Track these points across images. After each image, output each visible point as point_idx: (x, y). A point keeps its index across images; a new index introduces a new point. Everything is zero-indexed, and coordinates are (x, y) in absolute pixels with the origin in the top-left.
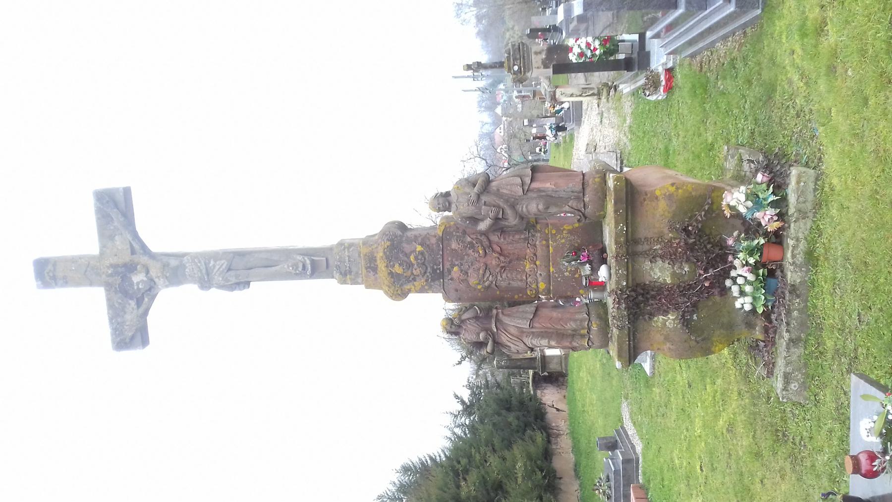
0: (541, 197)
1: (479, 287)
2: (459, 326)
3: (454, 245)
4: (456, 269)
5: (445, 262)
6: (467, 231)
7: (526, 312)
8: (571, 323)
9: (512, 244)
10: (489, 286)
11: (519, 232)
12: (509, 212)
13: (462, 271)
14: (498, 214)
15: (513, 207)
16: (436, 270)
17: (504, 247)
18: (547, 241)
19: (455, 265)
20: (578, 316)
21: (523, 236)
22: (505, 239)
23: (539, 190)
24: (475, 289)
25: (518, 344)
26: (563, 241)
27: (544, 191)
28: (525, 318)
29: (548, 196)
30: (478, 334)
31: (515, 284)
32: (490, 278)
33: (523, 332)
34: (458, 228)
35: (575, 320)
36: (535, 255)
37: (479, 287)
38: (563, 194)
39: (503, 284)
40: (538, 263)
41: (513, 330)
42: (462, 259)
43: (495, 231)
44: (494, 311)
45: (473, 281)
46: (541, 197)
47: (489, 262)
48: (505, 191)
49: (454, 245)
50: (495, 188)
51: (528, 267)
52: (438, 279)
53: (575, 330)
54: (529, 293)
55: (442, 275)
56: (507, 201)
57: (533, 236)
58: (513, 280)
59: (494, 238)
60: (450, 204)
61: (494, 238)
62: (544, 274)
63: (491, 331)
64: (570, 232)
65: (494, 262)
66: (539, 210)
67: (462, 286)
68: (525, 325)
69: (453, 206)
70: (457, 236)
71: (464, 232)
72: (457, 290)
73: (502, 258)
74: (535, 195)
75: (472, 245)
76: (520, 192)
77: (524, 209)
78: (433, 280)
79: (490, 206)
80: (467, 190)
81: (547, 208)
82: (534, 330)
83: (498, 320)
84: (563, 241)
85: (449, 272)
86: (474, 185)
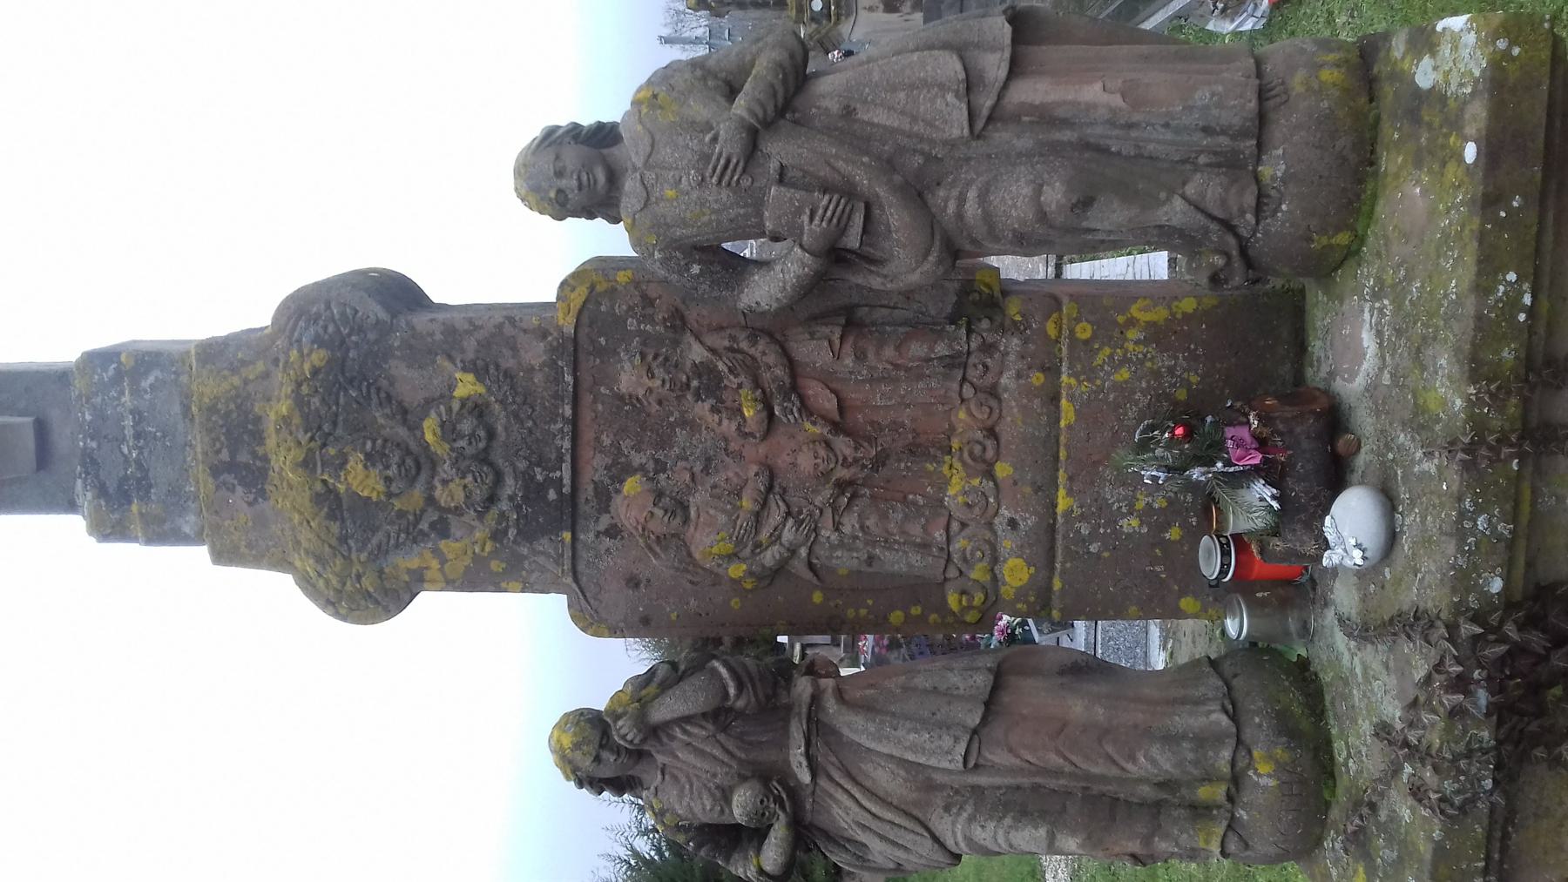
0: (1055, 149)
1: (736, 570)
2: (639, 755)
3: (629, 378)
4: (632, 485)
5: (586, 453)
6: (692, 315)
7: (950, 695)
8: (1155, 751)
9: (888, 383)
10: (780, 570)
11: (921, 327)
12: (896, 217)
13: (659, 495)
14: (843, 230)
15: (917, 193)
16: (541, 489)
17: (853, 395)
18: (1052, 371)
19: (628, 470)
20: (1183, 721)
21: (941, 349)
22: (860, 357)
23: (1046, 117)
24: (716, 579)
25: (906, 839)
26: (1124, 374)
27: (1065, 123)
28: (945, 726)
29: (1085, 145)
30: (725, 795)
31: (898, 562)
32: (788, 535)
33: (930, 787)
34: (648, 301)
35: (1170, 739)
36: (992, 433)
37: (736, 570)
38: (1158, 141)
39: (845, 562)
40: (1003, 470)
41: (884, 778)
42: (664, 442)
43: (815, 318)
44: (803, 687)
45: (707, 542)
46: (1055, 149)
47: (782, 461)
48: (880, 117)
49: (629, 378)
50: (833, 105)
51: (958, 486)
52: (552, 529)
53: (1166, 785)
54: (953, 601)
55: (569, 512)
56: (889, 165)
57: (988, 348)
58: (888, 544)
59: (813, 351)
60: (614, 178)
61: (813, 351)
62: (1028, 521)
63: (785, 776)
64: (1157, 335)
65: (806, 461)
66: (1042, 216)
67: (659, 566)
68: (945, 756)
69: (630, 185)
70: (646, 340)
71: (678, 322)
72: (633, 582)
73: (843, 445)
74: (1025, 142)
75: (709, 383)
76: (957, 125)
77: (972, 209)
78: (528, 533)
79: (808, 189)
80: (699, 109)
81: (1086, 203)
82: (982, 780)
83: (817, 728)
84: (1124, 374)
85: (604, 498)
86: (732, 91)
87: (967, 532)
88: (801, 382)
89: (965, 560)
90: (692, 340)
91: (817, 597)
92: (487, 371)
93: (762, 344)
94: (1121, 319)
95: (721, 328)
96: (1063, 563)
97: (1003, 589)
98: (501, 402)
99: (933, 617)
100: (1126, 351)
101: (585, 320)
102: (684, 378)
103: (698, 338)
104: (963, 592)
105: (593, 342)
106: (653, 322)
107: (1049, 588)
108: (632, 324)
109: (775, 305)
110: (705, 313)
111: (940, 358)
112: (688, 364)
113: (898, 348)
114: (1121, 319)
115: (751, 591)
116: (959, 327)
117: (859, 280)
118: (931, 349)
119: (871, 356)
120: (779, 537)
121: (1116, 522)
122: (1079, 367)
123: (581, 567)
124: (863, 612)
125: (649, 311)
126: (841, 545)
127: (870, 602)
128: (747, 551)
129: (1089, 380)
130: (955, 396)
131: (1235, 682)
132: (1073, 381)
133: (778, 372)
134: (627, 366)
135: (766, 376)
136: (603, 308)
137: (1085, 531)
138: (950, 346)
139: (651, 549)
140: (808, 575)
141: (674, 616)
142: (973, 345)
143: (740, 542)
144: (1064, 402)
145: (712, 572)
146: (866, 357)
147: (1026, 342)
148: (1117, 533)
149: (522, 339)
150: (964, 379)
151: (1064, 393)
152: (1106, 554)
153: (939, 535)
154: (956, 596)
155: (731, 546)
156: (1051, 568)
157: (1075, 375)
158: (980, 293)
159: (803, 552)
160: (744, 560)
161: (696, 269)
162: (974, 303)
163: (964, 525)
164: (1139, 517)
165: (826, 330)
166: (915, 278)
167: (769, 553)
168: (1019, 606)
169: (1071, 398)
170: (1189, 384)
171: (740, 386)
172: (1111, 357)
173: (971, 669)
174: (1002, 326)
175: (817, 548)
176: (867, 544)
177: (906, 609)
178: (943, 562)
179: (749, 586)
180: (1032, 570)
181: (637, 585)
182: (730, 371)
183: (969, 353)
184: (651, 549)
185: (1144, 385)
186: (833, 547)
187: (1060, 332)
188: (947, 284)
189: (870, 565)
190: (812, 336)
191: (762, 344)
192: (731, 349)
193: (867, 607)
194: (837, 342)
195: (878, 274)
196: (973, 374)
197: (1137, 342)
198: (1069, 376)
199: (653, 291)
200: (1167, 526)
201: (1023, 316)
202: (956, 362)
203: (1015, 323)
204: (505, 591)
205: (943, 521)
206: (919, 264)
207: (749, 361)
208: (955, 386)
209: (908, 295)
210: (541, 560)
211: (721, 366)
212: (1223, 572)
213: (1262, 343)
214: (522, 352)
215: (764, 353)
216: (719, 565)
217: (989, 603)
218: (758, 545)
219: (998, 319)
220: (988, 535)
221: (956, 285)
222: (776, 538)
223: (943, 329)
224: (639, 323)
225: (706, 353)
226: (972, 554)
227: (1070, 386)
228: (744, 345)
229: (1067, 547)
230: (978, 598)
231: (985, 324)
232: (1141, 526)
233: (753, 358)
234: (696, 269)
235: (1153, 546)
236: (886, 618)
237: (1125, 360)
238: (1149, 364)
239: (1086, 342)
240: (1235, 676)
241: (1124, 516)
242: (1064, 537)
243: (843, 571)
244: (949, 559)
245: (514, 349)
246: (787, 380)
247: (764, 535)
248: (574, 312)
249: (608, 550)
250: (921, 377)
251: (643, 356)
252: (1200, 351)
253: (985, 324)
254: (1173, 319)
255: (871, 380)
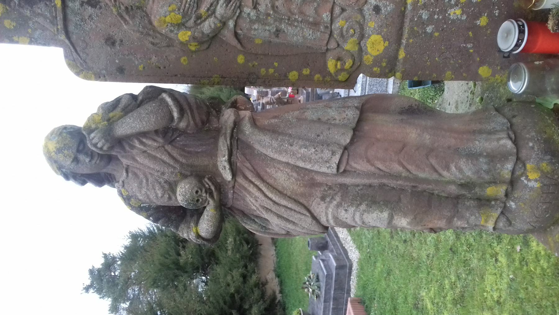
1: (184, 36)
2: (109, 159)
7: (329, 124)
8: (462, 163)
10: (214, 37)
20: (482, 144)
24: (170, 43)
25: (295, 217)
28: (326, 144)
30: (172, 187)
32: (220, 10)
33: (313, 184)
35: (472, 156)
37: (184, 36)
39: (260, 33)
41: (282, 178)
44: (228, 115)
53: (467, 185)
54: (331, 65)
58: (291, 22)
63: (215, 177)
68: (325, 164)
72: (110, 41)
82: (348, 180)
83: (237, 143)
87: (345, 14)
89: (342, 35)
91: (241, 59)
96: (408, 39)
97: (365, 57)
99: (317, 76)
104: (339, 59)
107: (396, 57)
115: (195, 52)
120: (214, 12)
121: (446, 11)
123: (71, 28)
124: (271, 71)
126: (258, 20)
127: (276, 64)
128: (191, 23)
131: (514, 120)
137: (425, 16)
139: (122, 17)
140: (234, 42)
141: (141, 68)
143: (185, 15)
145: (167, 37)
148: (446, 19)
152: (436, 34)
153: (326, 16)
154: (334, 61)
155: (180, 16)
156: (399, 43)
159: (231, 24)
160: (189, 29)
163: (343, 10)
164: (462, 8)
167: (207, 23)
168: (375, 69)
173: (344, 107)
175: (241, 21)
176: (275, 20)
177: (300, 71)
178: (327, 36)
179: (193, 49)
180: (387, 43)
181: (113, 44)
184: (122, 17)
186: (252, 22)
189: (277, 36)
193: (274, 67)
200: (478, 16)
204: (17, 42)
205: (329, 6)
210: (40, 20)
212: (517, 45)
216: (171, 31)
217: (355, 67)
218: (199, 17)
220: (359, 17)
222: (211, 12)
226: (347, 31)
229: (412, 28)
230: (348, 64)
232: (462, 14)
235: (469, 29)
236: (286, 76)
240: (514, 116)
241: (452, 7)
242: (412, 20)
243: (258, 41)
244: (331, 35)
247: (203, 10)
249: (90, 16)
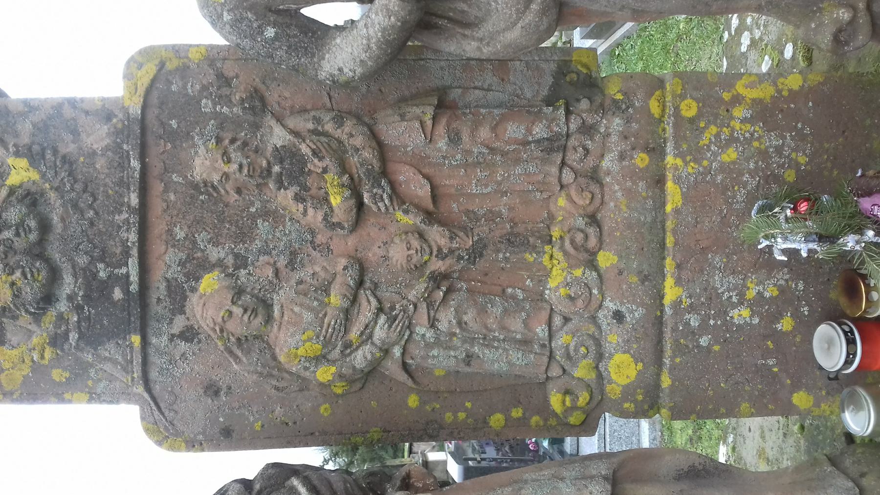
1: (325, 374)
3: (204, 163)
4: (209, 282)
5: (157, 247)
6: (273, 97)
9: (484, 166)
10: (372, 371)
13: (239, 292)
16: (105, 287)
17: (448, 182)
18: (656, 151)
19: (206, 266)
21: (539, 131)
22: (454, 139)
24: (304, 384)
31: (498, 360)
32: (380, 333)
34: (224, 80)
36: (593, 219)
37: (325, 374)
39: (441, 362)
40: (606, 259)
42: (244, 235)
45: (292, 342)
47: (373, 254)
49: (204, 163)
51: (559, 277)
52: (119, 332)
54: (556, 401)
55: (139, 312)
57: (588, 130)
58: (487, 342)
59: (404, 132)
61: (404, 132)
62: (635, 314)
64: (765, 113)
65: (398, 254)
67: (241, 371)
70: (222, 122)
71: (258, 104)
72: (212, 390)
73: (437, 235)
75: (292, 169)
78: (91, 337)
85: (178, 298)
87: (570, 326)
88: (392, 167)
89: (568, 357)
90: (273, 123)
91: (413, 401)
92: (43, 157)
93: (349, 125)
94: (726, 96)
95: (304, 111)
96: (672, 358)
97: (608, 388)
98: (57, 189)
99: (535, 419)
100: (733, 130)
101: (154, 100)
102: (264, 163)
103: (279, 120)
104: (567, 392)
105: (163, 124)
106: (230, 103)
107: (657, 386)
108: (207, 105)
109: (359, 71)
110: (287, 94)
111: (538, 142)
112: (270, 149)
113: (494, 129)
114: (726, 96)
115: (342, 395)
116: (556, 109)
117: (450, 47)
118: (529, 131)
119: (465, 137)
120: (371, 336)
121: (726, 313)
122: (685, 146)
123: (153, 374)
124: (462, 415)
125: (225, 91)
126: (438, 343)
127: (468, 405)
128: (336, 354)
129: (695, 160)
130: (554, 180)
131: (865, 482)
132: (679, 162)
133: (367, 154)
134: (202, 151)
135: (354, 160)
136: (174, 88)
137: (694, 322)
138: (549, 127)
139: (231, 352)
140: (402, 377)
141: (258, 426)
142: (573, 126)
143: (327, 343)
144: (670, 185)
145: (299, 377)
146: (460, 139)
147: (628, 121)
148: (728, 325)
149: (82, 119)
150: (563, 163)
151: (669, 176)
152: (716, 348)
153: (541, 331)
154: (559, 396)
155: (320, 347)
156: (659, 363)
157: (680, 155)
158: (578, 73)
159: (397, 351)
160: (333, 362)
161: (270, 32)
162: (571, 83)
163: (566, 320)
164: (750, 306)
165: (417, 111)
166: (514, 35)
167: (360, 352)
168: (626, 405)
169: (678, 180)
170: (798, 164)
171: (325, 170)
172: (717, 136)
173: (584, 478)
174: (602, 106)
175: (411, 347)
176: (464, 341)
177: (506, 412)
178: (545, 359)
179: (339, 391)
180: (640, 366)
181: (217, 393)
182: (314, 153)
183: (568, 136)
184: (231, 352)
185: (752, 166)
186: (429, 346)
187: (663, 110)
188: (544, 65)
189: (468, 364)
190: (403, 117)
191: (349, 125)
192: (315, 132)
193: (466, 410)
194: (429, 123)
195: (473, 39)
196: (573, 157)
197: (744, 121)
198: (676, 156)
199: (229, 69)
200: (778, 317)
201: (625, 94)
202: (555, 145)
203: (615, 101)
204: (70, 401)
205: (544, 315)
206: (521, 13)
207: (334, 145)
208: (554, 170)
209: (501, 65)
210: (108, 367)
211: (304, 149)
212: (848, 362)
213: (868, 122)
214: (83, 136)
215: (351, 135)
216: (306, 369)
217: (595, 401)
218: (348, 345)
219: (598, 100)
220: (592, 329)
221: (553, 66)
222: (367, 336)
223: (540, 111)
224: (215, 104)
225: (289, 137)
226: (576, 350)
227: (676, 168)
228: (329, 127)
229: (676, 341)
230: (583, 398)
231: (584, 104)
232: (751, 316)
233: (340, 142)
234: (270, 32)
235: (766, 337)
236: (485, 422)
237: (732, 140)
238: (756, 144)
239: (692, 121)
240: (863, 475)
241: (734, 306)
242: (674, 329)
243: (439, 373)
244: (551, 357)
245: (75, 133)
246: (376, 164)
247: (354, 334)
248: (141, 91)
249: (183, 355)
250: (517, 161)
251: (219, 141)
252: (807, 131)
253: (584, 104)
254: (778, 98)
255: (466, 166)
